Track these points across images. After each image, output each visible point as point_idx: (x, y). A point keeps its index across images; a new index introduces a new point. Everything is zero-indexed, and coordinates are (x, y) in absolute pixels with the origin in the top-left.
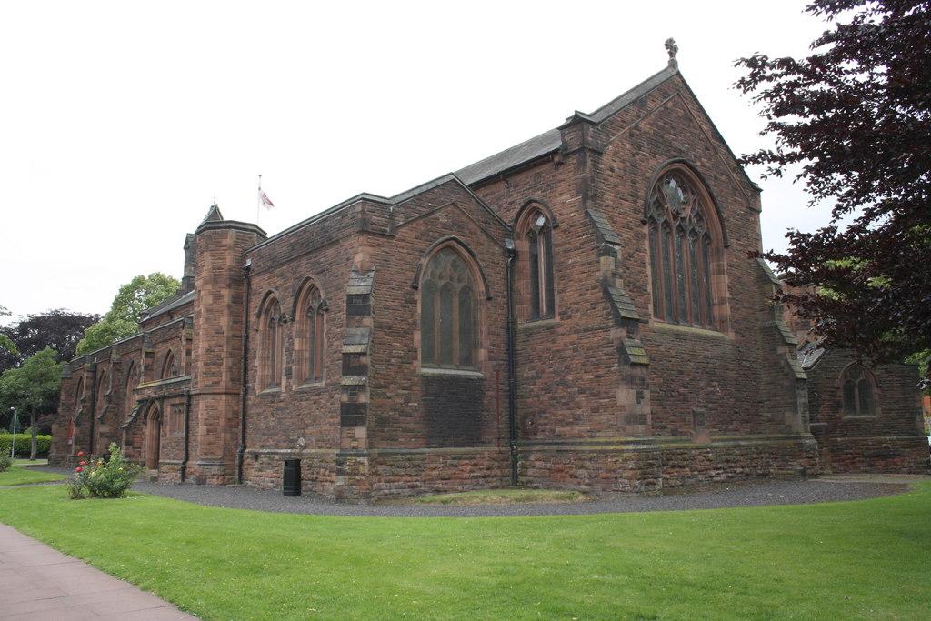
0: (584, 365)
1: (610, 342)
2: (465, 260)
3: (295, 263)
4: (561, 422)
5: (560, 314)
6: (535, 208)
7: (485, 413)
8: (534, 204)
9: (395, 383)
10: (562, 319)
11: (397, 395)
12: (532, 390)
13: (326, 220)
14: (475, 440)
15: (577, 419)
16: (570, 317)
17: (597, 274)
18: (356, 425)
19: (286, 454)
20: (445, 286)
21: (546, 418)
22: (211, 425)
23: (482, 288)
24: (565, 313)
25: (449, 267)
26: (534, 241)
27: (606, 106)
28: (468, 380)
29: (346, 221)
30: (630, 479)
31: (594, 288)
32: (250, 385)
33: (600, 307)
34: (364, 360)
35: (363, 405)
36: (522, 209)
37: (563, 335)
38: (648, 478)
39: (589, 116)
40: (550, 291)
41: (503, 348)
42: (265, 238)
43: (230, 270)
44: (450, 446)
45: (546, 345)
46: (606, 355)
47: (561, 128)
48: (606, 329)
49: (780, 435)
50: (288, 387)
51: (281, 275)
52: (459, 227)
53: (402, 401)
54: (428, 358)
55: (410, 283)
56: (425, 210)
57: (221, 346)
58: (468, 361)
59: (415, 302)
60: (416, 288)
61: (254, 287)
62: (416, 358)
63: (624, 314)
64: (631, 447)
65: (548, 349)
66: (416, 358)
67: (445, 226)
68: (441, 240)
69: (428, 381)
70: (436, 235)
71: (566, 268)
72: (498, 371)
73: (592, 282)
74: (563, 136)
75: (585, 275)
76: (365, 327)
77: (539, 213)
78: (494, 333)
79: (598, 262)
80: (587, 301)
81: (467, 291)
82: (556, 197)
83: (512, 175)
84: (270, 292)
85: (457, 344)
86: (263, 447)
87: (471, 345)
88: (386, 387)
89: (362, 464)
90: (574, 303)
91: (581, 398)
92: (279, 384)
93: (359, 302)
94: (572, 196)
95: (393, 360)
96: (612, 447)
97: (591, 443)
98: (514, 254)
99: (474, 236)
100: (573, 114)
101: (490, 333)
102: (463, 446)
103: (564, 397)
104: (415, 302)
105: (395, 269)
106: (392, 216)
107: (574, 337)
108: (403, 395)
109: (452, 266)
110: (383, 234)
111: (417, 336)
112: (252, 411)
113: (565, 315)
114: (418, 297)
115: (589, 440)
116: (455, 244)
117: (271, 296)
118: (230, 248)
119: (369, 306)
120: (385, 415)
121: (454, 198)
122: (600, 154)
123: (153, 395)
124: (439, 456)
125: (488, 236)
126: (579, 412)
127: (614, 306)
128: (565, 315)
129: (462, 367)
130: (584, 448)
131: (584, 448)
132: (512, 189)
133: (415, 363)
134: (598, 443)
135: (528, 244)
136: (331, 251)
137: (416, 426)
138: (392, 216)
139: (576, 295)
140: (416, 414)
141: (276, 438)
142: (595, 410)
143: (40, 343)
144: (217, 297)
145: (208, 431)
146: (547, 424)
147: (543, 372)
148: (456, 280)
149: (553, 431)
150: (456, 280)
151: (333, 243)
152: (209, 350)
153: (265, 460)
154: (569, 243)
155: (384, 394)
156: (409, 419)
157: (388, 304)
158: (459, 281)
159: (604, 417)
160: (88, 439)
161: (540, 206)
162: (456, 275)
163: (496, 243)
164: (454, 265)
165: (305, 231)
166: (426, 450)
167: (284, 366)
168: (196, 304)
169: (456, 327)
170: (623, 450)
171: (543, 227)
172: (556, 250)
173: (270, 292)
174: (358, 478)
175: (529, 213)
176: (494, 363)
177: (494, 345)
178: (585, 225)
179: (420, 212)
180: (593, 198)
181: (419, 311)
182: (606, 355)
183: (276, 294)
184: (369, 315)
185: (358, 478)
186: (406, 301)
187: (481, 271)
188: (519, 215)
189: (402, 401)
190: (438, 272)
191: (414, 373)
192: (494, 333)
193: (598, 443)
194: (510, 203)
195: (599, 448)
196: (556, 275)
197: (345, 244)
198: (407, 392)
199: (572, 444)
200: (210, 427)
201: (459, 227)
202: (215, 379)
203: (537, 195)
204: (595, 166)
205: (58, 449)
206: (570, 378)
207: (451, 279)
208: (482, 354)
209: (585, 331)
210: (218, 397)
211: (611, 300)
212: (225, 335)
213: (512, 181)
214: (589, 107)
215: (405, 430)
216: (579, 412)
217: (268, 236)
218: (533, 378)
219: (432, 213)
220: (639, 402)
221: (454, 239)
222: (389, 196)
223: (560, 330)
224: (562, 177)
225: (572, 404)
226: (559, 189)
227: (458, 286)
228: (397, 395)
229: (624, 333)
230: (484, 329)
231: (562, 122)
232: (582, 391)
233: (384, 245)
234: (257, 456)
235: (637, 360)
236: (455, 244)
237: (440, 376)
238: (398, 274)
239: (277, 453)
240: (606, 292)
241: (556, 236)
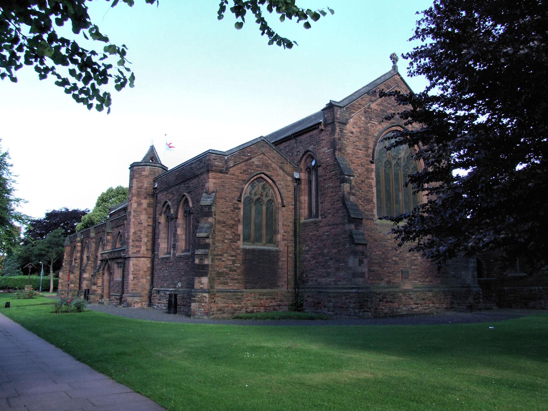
0: (332, 244)
1: (345, 231)
2: (270, 185)
3: (177, 187)
4: (320, 276)
5: (321, 215)
6: (310, 155)
7: (280, 270)
8: (309, 153)
9: (227, 253)
10: (322, 218)
11: (228, 260)
12: (306, 258)
13: (192, 164)
14: (273, 285)
15: (328, 274)
16: (325, 217)
17: (340, 193)
18: (202, 276)
19: (172, 291)
20: (258, 199)
21: (313, 273)
22: (135, 274)
23: (280, 201)
24: (323, 215)
25: (260, 188)
26: (310, 173)
27: (350, 96)
28: (269, 251)
29: (202, 164)
30: (353, 308)
31: (338, 201)
32: (156, 253)
33: (340, 212)
34: (207, 241)
35: (207, 266)
36: (304, 155)
37: (322, 227)
38: (364, 308)
39: (339, 103)
40: (317, 201)
41: (292, 233)
42: (167, 171)
43: (146, 189)
44: (258, 288)
45: (315, 233)
46: (343, 238)
47: (323, 110)
48: (344, 224)
49: (328, 291)
50: (174, 254)
51: (172, 193)
52: (266, 166)
53: (231, 263)
54: (247, 239)
55: (236, 198)
56: (247, 158)
57: (141, 231)
58: (271, 241)
59: (239, 209)
60: (240, 201)
61: (159, 198)
62: (239, 240)
63: (352, 216)
64: (354, 291)
65: (315, 235)
66: (239, 240)
67: (258, 166)
68: (255, 174)
69: (246, 251)
70: (253, 171)
71: (325, 190)
72: (288, 247)
73: (336, 198)
74: (324, 114)
75: (334, 194)
76: (209, 223)
77: (313, 158)
78: (286, 225)
79: (340, 186)
80: (335, 208)
81: (271, 201)
82: (320, 149)
83: (298, 136)
84: (166, 202)
85: (264, 231)
86: (161, 287)
87: (272, 230)
88: (222, 255)
89: (205, 297)
90: (328, 209)
91: (331, 263)
92: (170, 253)
93: (206, 209)
94: (329, 149)
95: (226, 241)
96: (344, 291)
97: (335, 288)
98: (298, 181)
99: (275, 171)
100: (329, 102)
101: (283, 225)
102: (266, 288)
103: (322, 262)
104: (239, 209)
105: (228, 191)
106: (226, 162)
107: (327, 228)
108: (232, 259)
109: (262, 188)
110: (221, 172)
111: (240, 227)
112: (157, 267)
113: (324, 216)
114: (241, 206)
115: (334, 286)
116: (263, 176)
117: (167, 204)
118: (146, 177)
119: (212, 212)
120: (221, 271)
121: (263, 150)
122: (345, 124)
123: (107, 257)
124: (252, 293)
125: (283, 171)
126: (329, 270)
127: (347, 211)
128: (324, 216)
129: (267, 244)
130: (331, 291)
131: (331, 291)
132: (299, 144)
133: (239, 242)
134: (339, 288)
135: (307, 175)
136: (195, 181)
137: (239, 277)
138: (226, 162)
139: (329, 205)
140: (239, 271)
141: (168, 282)
142: (338, 269)
143: (56, 225)
144: (139, 204)
145: (134, 278)
146: (313, 277)
147: (312, 247)
148: (264, 196)
149: (316, 281)
150: (264, 196)
151: (196, 176)
152: (135, 233)
153: (162, 294)
154: (326, 175)
155: (220, 259)
156: (234, 273)
157: (223, 210)
158: (267, 196)
159: (342, 274)
160: (78, 281)
161: (312, 154)
162: (265, 193)
163: (288, 174)
164: (264, 187)
165: (183, 169)
166: (244, 290)
167: (172, 243)
168: (129, 207)
169: (264, 223)
170: (350, 292)
171: (314, 166)
172: (320, 179)
173: (166, 202)
174: (203, 304)
175: (307, 158)
176: (286, 242)
177: (285, 232)
178: (335, 165)
179: (242, 159)
180: (340, 150)
181: (242, 213)
182: (343, 238)
183: (170, 203)
184: (211, 216)
185: (203, 304)
186: (234, 208)
187: (279, 190)
188: (302, 158)
189: (231, 263)
190: (254, 191)
191: (238, 248)
192: (286, 225)
193: (339, 288)
194: (298, 152)
195: (339, 291)
196: (320, 193)
197: (202, 177)
198: (233, 258)
199: (325, 288)
200: (135, 276)
201: (266, 166)
202: (138, 249)
203: (311, 148)
204: (341, 131)
205: (62, 286)
206: (325, 251)
207: (262, 195)
208: (279, 237)
209: (333, 225)
210: (139, 259)
211: (346, 208)
212: (143, 225)
213: (299, 139)
214: (338, 98)
215: (232, 279)
216: (329, 270)
217: (126, 185)
218: (307, 251)
219: (250, 159)
220: (360, 265)
221: (263, 173)
222: (225, 151)
223: (321, 224)
224: (323, 138)
225: (326, 266)
226: (322, 145)
227: (265, 199)
228: (228, 260)
229: (353, 226)
230: (280, 223)
231: (324, 106)
232: (331, 259)
233: (221, 178)
234: (158, 292)
235: (358, 242)
236: (263, 176)
237: (253, 250)
238: (229, 193)
239: (168, 291)
240: (344, 204)
241: (320, 170)
